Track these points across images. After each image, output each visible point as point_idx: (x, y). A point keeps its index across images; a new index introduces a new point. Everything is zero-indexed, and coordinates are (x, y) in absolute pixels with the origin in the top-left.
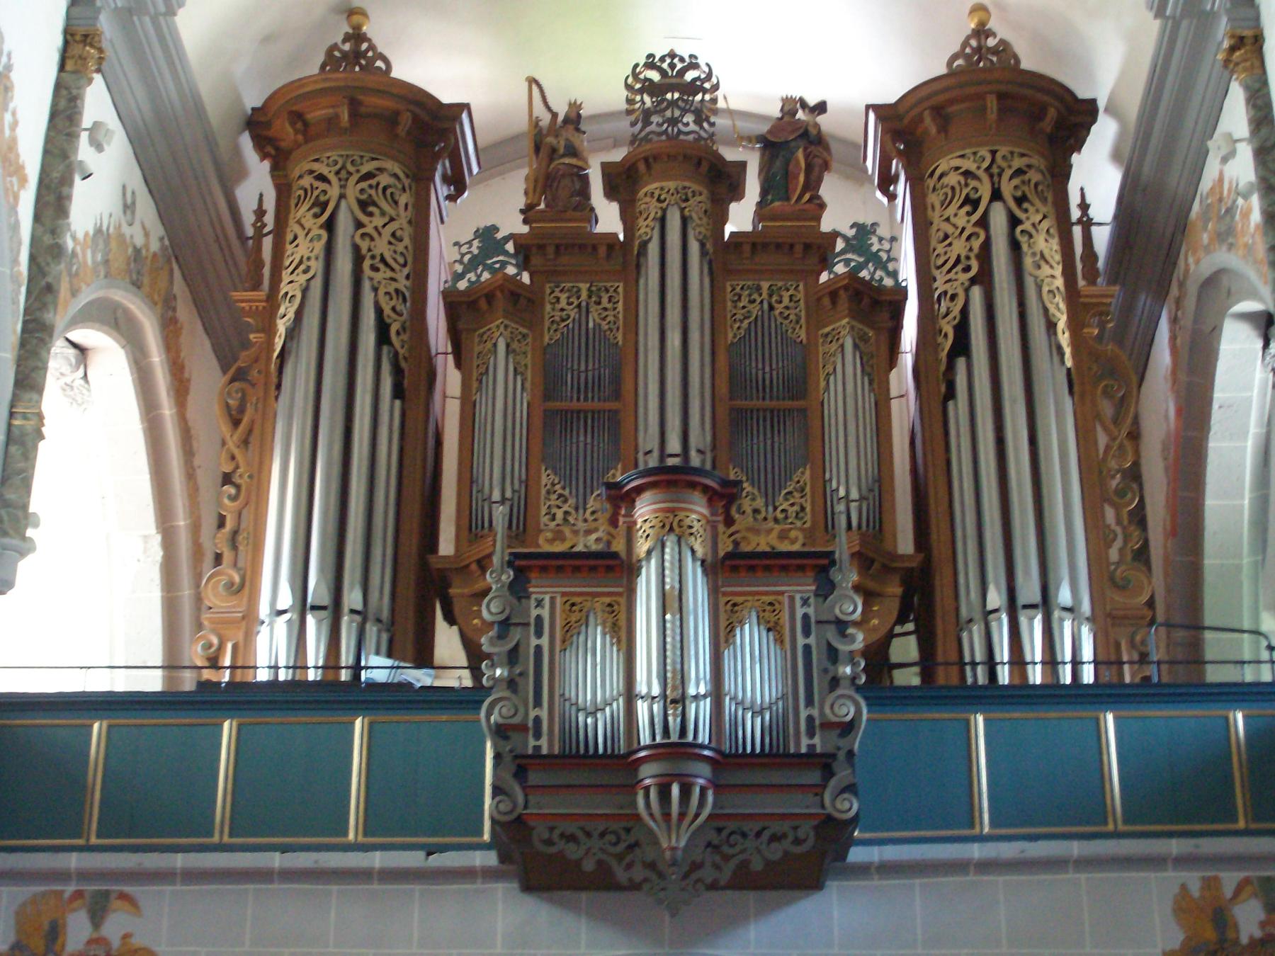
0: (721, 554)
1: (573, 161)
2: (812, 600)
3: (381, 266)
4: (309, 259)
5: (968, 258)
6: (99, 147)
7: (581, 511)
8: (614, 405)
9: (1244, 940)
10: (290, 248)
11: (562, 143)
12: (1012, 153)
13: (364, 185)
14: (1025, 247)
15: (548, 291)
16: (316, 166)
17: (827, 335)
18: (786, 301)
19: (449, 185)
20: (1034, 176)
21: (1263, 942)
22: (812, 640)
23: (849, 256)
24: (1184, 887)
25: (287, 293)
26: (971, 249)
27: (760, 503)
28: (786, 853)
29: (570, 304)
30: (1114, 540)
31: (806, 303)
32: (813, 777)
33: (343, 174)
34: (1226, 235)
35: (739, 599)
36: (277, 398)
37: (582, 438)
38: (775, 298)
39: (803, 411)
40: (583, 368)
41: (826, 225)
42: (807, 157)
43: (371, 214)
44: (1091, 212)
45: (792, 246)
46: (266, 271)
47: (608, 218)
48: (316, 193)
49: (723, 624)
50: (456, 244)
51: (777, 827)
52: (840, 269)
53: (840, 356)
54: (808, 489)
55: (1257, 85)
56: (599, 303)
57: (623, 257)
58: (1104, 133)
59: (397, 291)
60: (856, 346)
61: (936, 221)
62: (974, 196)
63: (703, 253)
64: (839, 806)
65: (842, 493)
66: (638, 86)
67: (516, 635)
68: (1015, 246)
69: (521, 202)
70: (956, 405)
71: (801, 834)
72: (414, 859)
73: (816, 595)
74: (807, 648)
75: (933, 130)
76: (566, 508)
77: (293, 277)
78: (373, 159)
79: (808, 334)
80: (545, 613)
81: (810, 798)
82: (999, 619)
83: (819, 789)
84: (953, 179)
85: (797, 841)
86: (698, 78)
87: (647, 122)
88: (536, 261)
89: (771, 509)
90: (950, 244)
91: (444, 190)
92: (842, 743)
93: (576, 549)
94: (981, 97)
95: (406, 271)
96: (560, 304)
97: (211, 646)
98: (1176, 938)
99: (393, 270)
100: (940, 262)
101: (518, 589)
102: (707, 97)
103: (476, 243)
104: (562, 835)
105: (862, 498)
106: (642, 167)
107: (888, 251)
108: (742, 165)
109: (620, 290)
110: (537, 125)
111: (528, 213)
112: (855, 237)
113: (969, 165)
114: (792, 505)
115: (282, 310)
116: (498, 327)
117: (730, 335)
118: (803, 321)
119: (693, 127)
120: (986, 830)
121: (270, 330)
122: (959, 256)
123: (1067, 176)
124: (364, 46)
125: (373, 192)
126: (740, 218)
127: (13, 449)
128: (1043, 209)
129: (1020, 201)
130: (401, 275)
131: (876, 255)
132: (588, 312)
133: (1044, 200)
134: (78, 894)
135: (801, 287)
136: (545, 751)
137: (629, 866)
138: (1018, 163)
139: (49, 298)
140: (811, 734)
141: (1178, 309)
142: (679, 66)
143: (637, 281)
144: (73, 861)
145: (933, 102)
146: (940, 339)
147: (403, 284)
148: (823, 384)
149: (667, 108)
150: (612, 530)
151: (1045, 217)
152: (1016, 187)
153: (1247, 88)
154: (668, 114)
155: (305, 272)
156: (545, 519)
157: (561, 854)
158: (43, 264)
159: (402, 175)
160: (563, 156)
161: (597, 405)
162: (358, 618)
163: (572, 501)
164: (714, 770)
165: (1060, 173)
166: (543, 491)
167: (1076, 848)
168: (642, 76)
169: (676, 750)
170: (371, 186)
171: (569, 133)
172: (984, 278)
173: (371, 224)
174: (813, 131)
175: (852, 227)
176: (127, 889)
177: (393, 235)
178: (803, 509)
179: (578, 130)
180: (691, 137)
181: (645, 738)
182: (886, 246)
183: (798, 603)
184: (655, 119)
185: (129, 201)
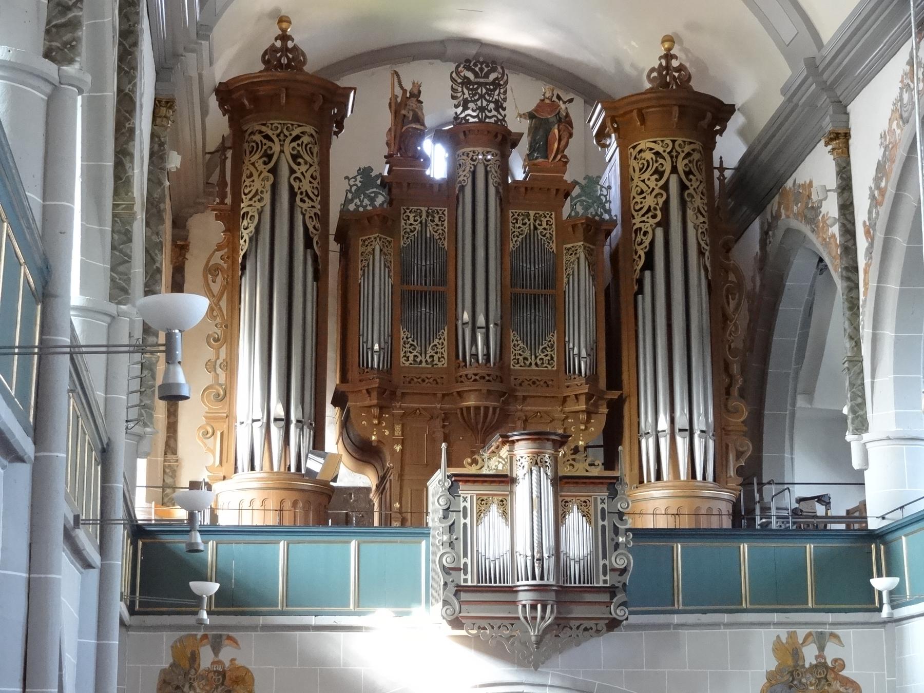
1: (418, 127)
3: (306, 199)
4: (262, 192)
5: (655, 209)
8: (441, 289)
9: (807, 665)
11: (411, 113)
13: (294, 144)
14: (689, 204)
15: (403, 211)
16: (264, 129)
17: (568, 249)
20: (696, 156)
21: (816, 666)
22: (606, 523)
23: (583, 198)
24: (778, 637)
25: (248, 213)
26: (657, 204)
27: (527, 354)
29: (415, 221)
31: (556, 226)
32: (605, 598)
33: (282, 137)
35: (568, 499)
38: (538, 222)
40: (424, 263)
41: (568, 177)
42: (559, 131)
43: (299, 164)
46: (228, 189)
48: (265, 147)
49: (560, 512)
51: (587, 624)
53: (576, 263)
57: (447, 193)
58: (736, 121)
59: (315, 214)
62: (661, 169)
63: (497, 192)
64: (618, 611)
65: (576, 351)
66: (459, 81)
67: (453, 517)
68: (683, 204)
69: (386, 151)
70: (643, 299)
74: (603, 526)
76: (415, 353)
78: (299, 126)
80: (468, 505)
81: (603, 608)
83: (608, 604)
84: (648, 155)
86: (497, 79)
87: (466, 108)
90: (644, 198)
92: (620, 578)
96: (410, 222)
99: (312, 200)
100: (637, 208)
101: (452, 490)
102: (502, 91)
103: (359, 178)
105: (588, 355)
106: (462, 136)
107: (605, 196)
108: (521, 135)
109: (446, 213)
111: (389, 158)
112: (587, 186)
113: (658, 148)
114: (546, 355)
116: (375, 238)
117: (511, 245)
118: (554, 238)
119: (494, 113)
122: (650, 207)
124: (290, 44)
125: (299, 149)
127: (145, 372)
128: (700, 177)
129: (687, 174)
132: (426, 226)
133: (700, 170)
134: (205, 637)
135: (553, 216)
136: (469, 584)
138: (687, 149)
140: (605, 574)
142: (486, 70)
145: (640, 105)
146: (636, 257)
148: (565, 280)
149: (478, 100)
151: (701, 182)
153: (838, 165)
155: (259, 201)
156: (403, 360)
158: (153, 254)
159: (314, 134)
160: (411, 122)
163: (418, 349)
165: (710, 146)
167: (726, 618)
168: (462, 74)
170: (298, 145)
172: (665, 223)
176: (231, 634)
177: (312, 176)
178: (552, 358)
184: (471, 105)
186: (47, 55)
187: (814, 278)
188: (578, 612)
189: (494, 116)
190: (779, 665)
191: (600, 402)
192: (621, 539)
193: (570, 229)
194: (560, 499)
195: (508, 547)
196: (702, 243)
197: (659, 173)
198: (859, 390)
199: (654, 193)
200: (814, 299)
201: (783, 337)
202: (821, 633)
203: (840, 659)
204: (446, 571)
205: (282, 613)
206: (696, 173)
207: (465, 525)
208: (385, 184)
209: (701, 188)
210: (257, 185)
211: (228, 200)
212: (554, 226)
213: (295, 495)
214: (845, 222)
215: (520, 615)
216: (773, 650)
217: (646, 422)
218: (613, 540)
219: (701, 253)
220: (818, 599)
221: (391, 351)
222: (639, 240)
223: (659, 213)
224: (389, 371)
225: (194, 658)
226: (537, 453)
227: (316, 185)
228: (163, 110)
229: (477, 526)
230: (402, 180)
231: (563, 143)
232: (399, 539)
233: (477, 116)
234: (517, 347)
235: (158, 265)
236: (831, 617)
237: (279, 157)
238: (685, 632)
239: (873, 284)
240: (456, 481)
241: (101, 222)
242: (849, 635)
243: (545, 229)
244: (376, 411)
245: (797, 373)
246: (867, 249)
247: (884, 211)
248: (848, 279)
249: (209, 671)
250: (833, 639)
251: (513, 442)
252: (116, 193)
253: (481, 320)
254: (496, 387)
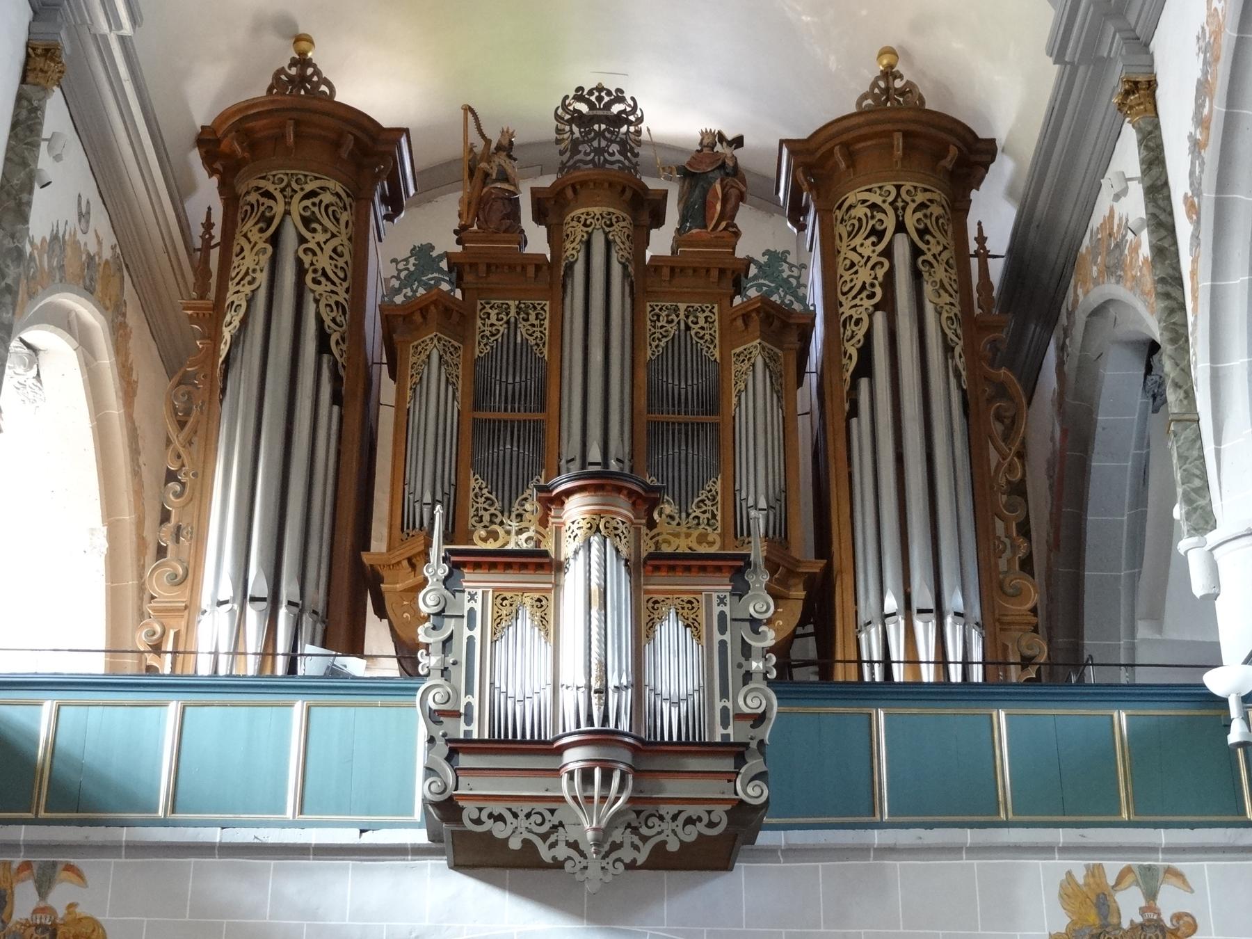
0: (644, 555)
1: (506, 186)
2: (728, 600)
3: (323, 279)
4: (254, 271)
5: (873, 285)
6: (58, 158)
7: (506, 514)
8: (538, 416)
9: (1126, 925)
10: (236, 261)
11: (495, 169)
12: (915, 188)
13: (308, 203)
14: (926, 275)
15: (479, 307)
16: (262, 183)
18: (702, 322)
19: (387, 205)
20: (936, 210)
23: (762, 281)
24: (1069, 873)
26: (875, 278)
28: (700, 835)
30: (1004, 551)
32: (727, 764)
34: (1115, 269)
35: (660, 597)
36: (221, 401)
37: (508, 446)
38: (691, 318)
39: (715, 426)
40: (510, 381)
41: (740, 253)
42: (723, 188)
43: (314, 231)
44: (988, 245)
45: (708, 271)
46: (213, 281)
47: (537, 241)
48: (262, 209)
49: (644, 619)
50: (392, 261)
52: (753, 293)
54: (719, 498)
55: (1150, 128)
56: (527, 320)
57: (551, 276)
58: (1002, 172)
59: (337, 303)
60: (766, 365)
61: (844, 250)
63: (626, 274)
64: (749, 790)
65: (751, 502)
67: (450, 625)
68: (917, 275)
69: (455, 223)
71: (715, 819)
72: (349, 836)
73: (732, 595)
74: (723, 644)
75: (843, 165)
76: (492, 510)
77: (239, 287)
78: (316, 178)
79: (721, 353)
80: (478, 607)
82: (897, 622)
83: (731, 776)
84: (861, 211)
85: (711, 825)
86: (624, 111)
88: (469, 278)
89: (684, 515)
90: (856, 272)
91: (382, 210)
92: (753, 732)
93: (509, 547)
94: (889, 134)
95: (346, 285)
96: (491, 320)
97: (154, 633)
98: (1062, 922)
99: (333, 283)
100: (845, 289)
102: (632, 129)
103: (412, 260)
104: (490, 816)
105: (770, 507)
106: (569, 193)
107: (798, 278)
109: (547, 308)
110: (471, 150)
111: (461, 234)
112: (766, 264)
113: (875, 198)
114: (704, 512)
115: (228, 318)
117: (649, 352)
118: (717, 341)
119: (618, 157)
120: (886, 817)
121: (216, 338)
123: (966, 211)
124: (310, 71)
125: (316, 209)
126: (660, 243)
128: (943, 241)
129: (922, 233)
130: (341, 290)
131: (786, 281)
134: (27, 866)
135: (715, 310)
136: (475, 736)
137: (553, 845)
138: (920, 197)
139: (8, 299)
140: (725, 725)
141: (1066, 337)
142: (607, 99)
143: (563, 299)
144: (22, 833)
145: (845, 137)
146: (845, 361)
147: (342, 297)
148: (734, 400)
149: (594, 139)
150: (541, 529)
151: (945, 248)
152: (919, 220)
153: (1139, 130)
154: (595, 144)
155: (250, 283)
157: (489, 833)
159: (343, 195)
161: (522, 416)
162: (296, 610)
164: (634, 757)
165: (959, 207)
166: (472, 494)
169: (602, 737)
170: (314, 204)
171: (501, 159)
172: (888, 305)
173: (313, 240)
174: (730, 163)
175: (764, 254)
176: (72, 861)
177: (335, 250)
178: (714, 516)
179: (510, 157)
180: (616, 167)
181: (571, 727)
182: (796, 273)
183: (715, 601)
184: (584, 148)
185: (84, 211)
187: (1144, 419)
188: (674, 788)
189: (619, 161)
190: (1073, 923)
191: (792, 582)
192: (754, 665)
193: (740, 322)
194: (644, 597)
195: (550, 680)
196: (947, 331)
197: (878, 234)
198: (1197, 468)
199: (870, 264)
200: (1148, 453)
201: (1105, 515)
202: (1149, 868)
203: (1187, 915)
205: (164, 823)
206: (937, 234)
207: (471, 639)
209: (945, 255)
210: (249, 261)
211: (212, 294)
212: (716, 324)
214: (1157, 212)
215: (565, 793)
216: (1061, 896)
217: (867, 607)
218: (740, 666)
219: (948, 349)
220: (1139, 805)
222: (848, 333)
223: (879, 291)
226: (599, 514)
227: (341, 263)
228: (40, 63)
229: (494, 642)
231: (729, 206)
232: (379, 700)
233: (592, 161)
235: (9, 281)
236: (1163, 837)
237: (283, 220)
238: (897, 866)
239: (1205, 284)
240: (458, 564)
242: (1200, 870)
243: (702, 328)
245: (1134, 579)
246: (1193, 235)
247: (1211, 154)
248: (1167, 296)
249: (26, 925)
250: (1173, 880)
251: (560, 500)
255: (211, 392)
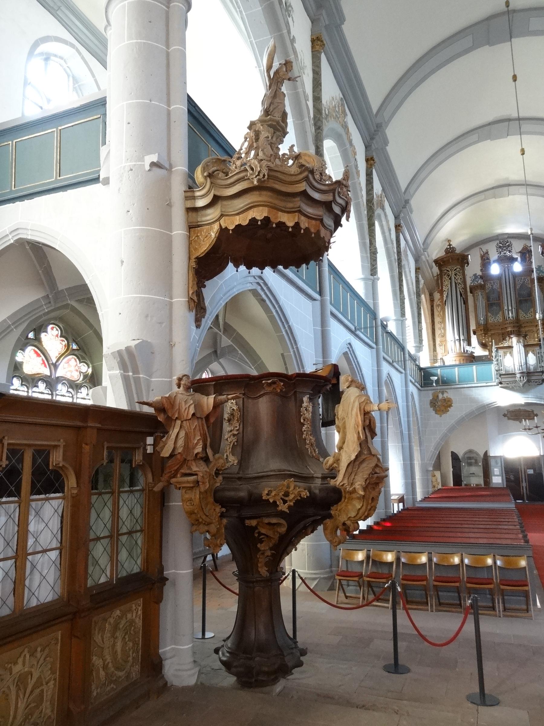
32: (541, 374)
67: (497, 357)
69: (480, 268)
72: (485, 384)
83: (542, 375)
96: (488, 286)
101: (497, 351)
186: (371, 275)
188: (533, 378)
204: (497, 371)
208: (481, 277)
210: (446, 283)
213: (463, 358)
221: (486, 319)
224: (486, 324)
225: (438, 396)
228: (418, 270)
230: (485, 277)
234: (522, 314)
240: (498, 349)
241: (397, 300)
244: (483, 335)
252: (400, 294)
253: (510, 308)
254: (517, 325)
255: (443, 304)
